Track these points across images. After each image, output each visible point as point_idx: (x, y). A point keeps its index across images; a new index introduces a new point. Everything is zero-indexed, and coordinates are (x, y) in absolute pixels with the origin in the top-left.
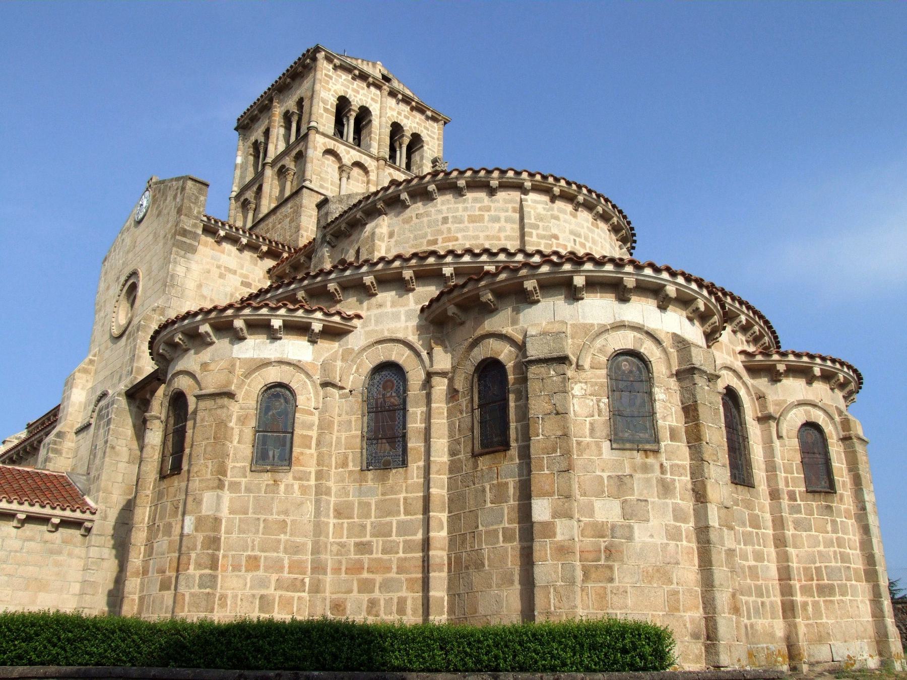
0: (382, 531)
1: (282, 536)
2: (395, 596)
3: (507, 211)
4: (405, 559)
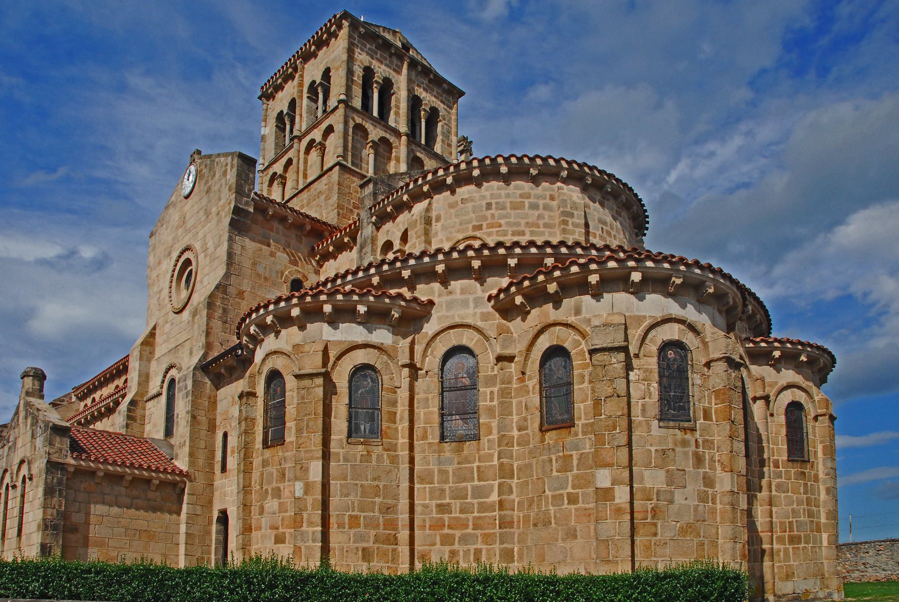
0: (460, 495)
1: (377, 499)
2: (472, 548)
3: (545, 199)
4: (480, 518)
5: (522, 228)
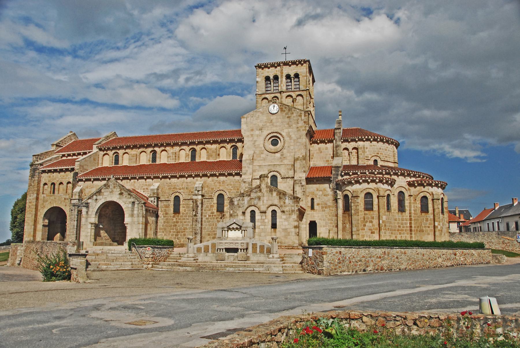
0: (402, 224)
2: (405, 235)
5: (387, 156)
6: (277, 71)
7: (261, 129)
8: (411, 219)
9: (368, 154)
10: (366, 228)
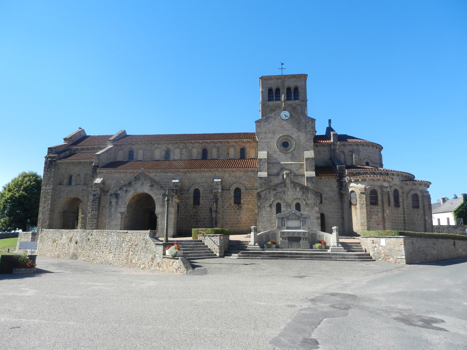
6: (278, 83)
7: (274, 133)
8: (404, 214)
9: (361, 157)
10: (372, 220)
